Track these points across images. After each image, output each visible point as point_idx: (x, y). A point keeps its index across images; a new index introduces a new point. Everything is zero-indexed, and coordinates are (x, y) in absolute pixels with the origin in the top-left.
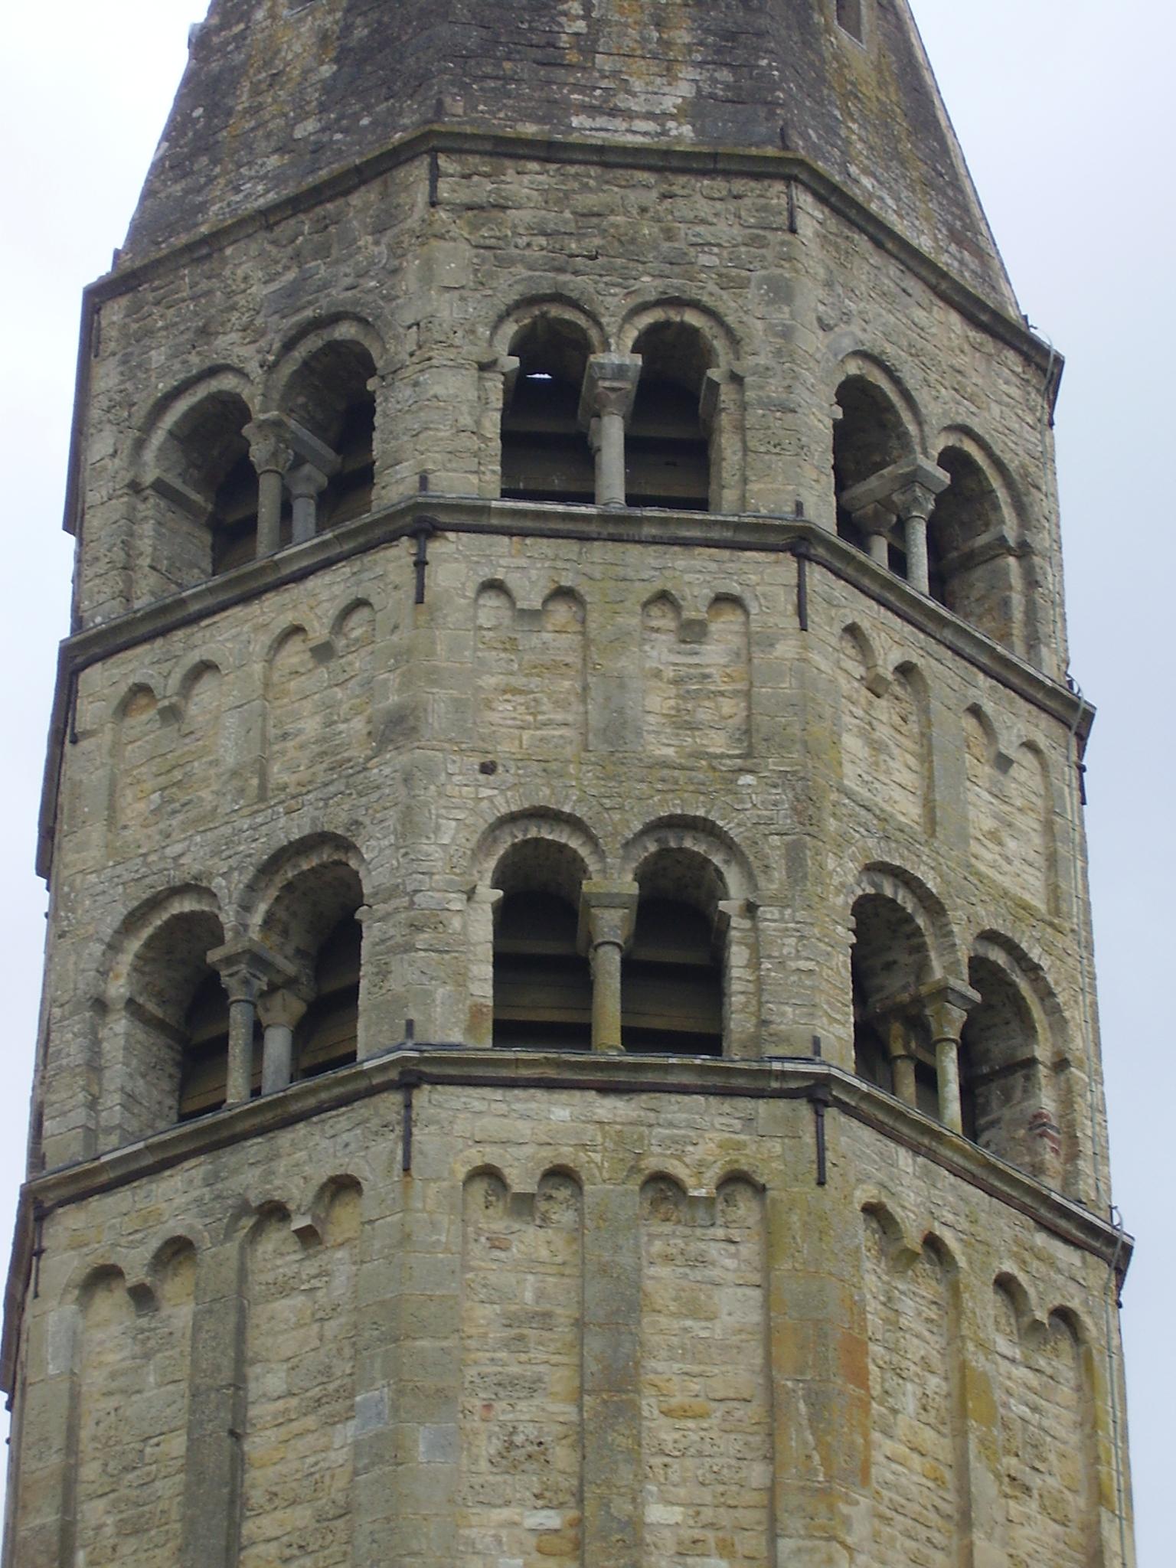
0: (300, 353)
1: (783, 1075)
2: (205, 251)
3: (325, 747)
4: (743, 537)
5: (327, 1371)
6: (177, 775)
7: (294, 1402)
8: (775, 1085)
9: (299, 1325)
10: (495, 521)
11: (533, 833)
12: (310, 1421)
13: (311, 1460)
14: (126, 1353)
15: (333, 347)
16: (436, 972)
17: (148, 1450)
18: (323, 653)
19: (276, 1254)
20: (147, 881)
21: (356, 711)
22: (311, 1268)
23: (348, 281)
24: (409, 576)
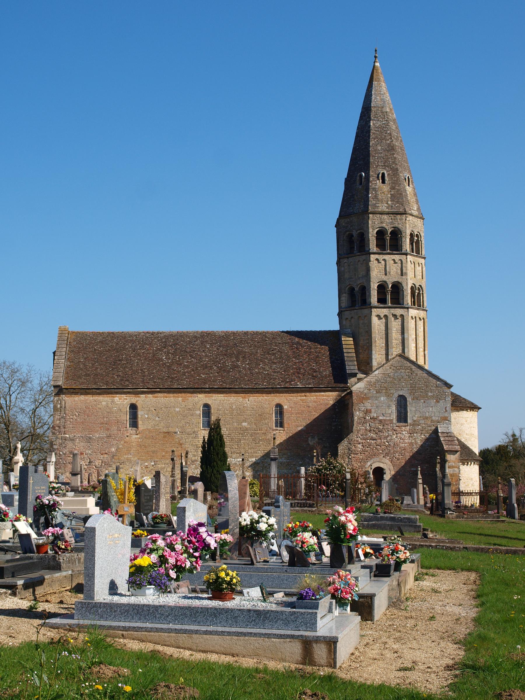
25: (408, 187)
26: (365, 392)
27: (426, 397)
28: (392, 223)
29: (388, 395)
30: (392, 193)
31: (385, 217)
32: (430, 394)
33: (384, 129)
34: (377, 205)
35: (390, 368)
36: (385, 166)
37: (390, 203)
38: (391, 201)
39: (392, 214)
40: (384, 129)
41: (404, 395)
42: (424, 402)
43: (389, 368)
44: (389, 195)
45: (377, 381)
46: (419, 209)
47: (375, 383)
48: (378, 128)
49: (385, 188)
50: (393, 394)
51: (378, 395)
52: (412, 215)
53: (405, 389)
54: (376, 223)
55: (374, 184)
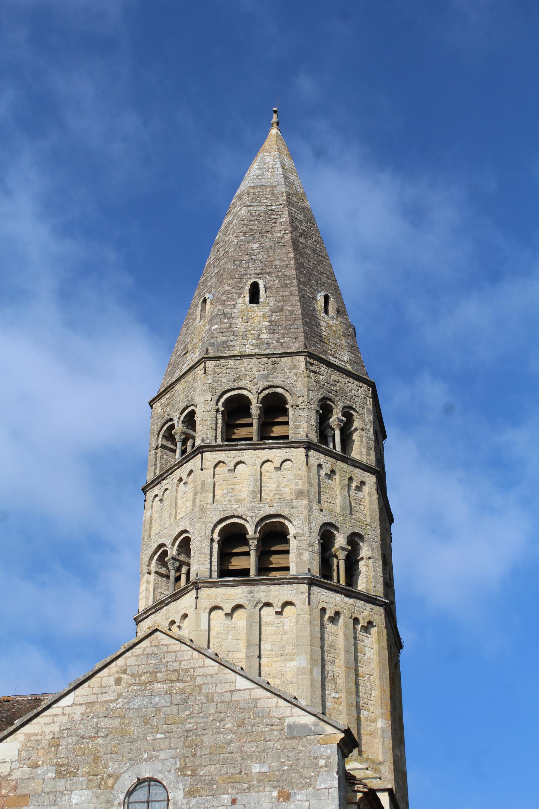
0: (266, 392)
1: (380, 600)
2: (239, 358)
3: (277, 492)
4: (366, 469)
5: (284, 648)
6: (232, 487)
7: (274, 653)
8: (377, 602)
9: (274, 634)
10: (321, 450)
11: (328, 528)
12: (279, 659)
13: (279, 668)
14: (222, 628)
15: (275, 393)
16: (301, 555)
17: (229, 655)
18: (278, 469)
19: (268, 614)
20: (226, 512)
21: (287, 486)
22: (277, 621)
23: (282, 379)
24: (304, 458)
25: (323, 314)
26: (16, 775)
27: (239, 780)
28: (265, 378)
29: (100, 783)
30: (273, 318)
31: (250, 363)
32: (256, 768)
33: (272, 217)
34: (231, 343)
35: (118, 681)
36: (262, 274)
37: (264, 336)
38: (268, 334)
39: (267, 355)
40: (272, 217)
41: (159, 777)
42: (234, 801)
43: (112, 680)
44: (267, 324)
45: (69, 730)
46: (357, 362)
47: (55, 743)
48: (259, 215)
49: (258, 311)
50: (118, 778)
51: (61, 784)
52: (329, 365)
53: (162, 755)
54: (224, 380)
55: (230, 305)
